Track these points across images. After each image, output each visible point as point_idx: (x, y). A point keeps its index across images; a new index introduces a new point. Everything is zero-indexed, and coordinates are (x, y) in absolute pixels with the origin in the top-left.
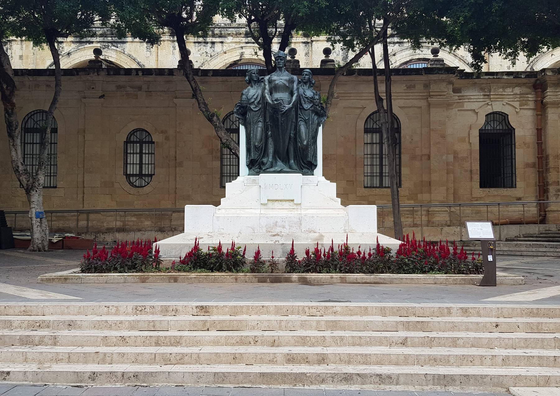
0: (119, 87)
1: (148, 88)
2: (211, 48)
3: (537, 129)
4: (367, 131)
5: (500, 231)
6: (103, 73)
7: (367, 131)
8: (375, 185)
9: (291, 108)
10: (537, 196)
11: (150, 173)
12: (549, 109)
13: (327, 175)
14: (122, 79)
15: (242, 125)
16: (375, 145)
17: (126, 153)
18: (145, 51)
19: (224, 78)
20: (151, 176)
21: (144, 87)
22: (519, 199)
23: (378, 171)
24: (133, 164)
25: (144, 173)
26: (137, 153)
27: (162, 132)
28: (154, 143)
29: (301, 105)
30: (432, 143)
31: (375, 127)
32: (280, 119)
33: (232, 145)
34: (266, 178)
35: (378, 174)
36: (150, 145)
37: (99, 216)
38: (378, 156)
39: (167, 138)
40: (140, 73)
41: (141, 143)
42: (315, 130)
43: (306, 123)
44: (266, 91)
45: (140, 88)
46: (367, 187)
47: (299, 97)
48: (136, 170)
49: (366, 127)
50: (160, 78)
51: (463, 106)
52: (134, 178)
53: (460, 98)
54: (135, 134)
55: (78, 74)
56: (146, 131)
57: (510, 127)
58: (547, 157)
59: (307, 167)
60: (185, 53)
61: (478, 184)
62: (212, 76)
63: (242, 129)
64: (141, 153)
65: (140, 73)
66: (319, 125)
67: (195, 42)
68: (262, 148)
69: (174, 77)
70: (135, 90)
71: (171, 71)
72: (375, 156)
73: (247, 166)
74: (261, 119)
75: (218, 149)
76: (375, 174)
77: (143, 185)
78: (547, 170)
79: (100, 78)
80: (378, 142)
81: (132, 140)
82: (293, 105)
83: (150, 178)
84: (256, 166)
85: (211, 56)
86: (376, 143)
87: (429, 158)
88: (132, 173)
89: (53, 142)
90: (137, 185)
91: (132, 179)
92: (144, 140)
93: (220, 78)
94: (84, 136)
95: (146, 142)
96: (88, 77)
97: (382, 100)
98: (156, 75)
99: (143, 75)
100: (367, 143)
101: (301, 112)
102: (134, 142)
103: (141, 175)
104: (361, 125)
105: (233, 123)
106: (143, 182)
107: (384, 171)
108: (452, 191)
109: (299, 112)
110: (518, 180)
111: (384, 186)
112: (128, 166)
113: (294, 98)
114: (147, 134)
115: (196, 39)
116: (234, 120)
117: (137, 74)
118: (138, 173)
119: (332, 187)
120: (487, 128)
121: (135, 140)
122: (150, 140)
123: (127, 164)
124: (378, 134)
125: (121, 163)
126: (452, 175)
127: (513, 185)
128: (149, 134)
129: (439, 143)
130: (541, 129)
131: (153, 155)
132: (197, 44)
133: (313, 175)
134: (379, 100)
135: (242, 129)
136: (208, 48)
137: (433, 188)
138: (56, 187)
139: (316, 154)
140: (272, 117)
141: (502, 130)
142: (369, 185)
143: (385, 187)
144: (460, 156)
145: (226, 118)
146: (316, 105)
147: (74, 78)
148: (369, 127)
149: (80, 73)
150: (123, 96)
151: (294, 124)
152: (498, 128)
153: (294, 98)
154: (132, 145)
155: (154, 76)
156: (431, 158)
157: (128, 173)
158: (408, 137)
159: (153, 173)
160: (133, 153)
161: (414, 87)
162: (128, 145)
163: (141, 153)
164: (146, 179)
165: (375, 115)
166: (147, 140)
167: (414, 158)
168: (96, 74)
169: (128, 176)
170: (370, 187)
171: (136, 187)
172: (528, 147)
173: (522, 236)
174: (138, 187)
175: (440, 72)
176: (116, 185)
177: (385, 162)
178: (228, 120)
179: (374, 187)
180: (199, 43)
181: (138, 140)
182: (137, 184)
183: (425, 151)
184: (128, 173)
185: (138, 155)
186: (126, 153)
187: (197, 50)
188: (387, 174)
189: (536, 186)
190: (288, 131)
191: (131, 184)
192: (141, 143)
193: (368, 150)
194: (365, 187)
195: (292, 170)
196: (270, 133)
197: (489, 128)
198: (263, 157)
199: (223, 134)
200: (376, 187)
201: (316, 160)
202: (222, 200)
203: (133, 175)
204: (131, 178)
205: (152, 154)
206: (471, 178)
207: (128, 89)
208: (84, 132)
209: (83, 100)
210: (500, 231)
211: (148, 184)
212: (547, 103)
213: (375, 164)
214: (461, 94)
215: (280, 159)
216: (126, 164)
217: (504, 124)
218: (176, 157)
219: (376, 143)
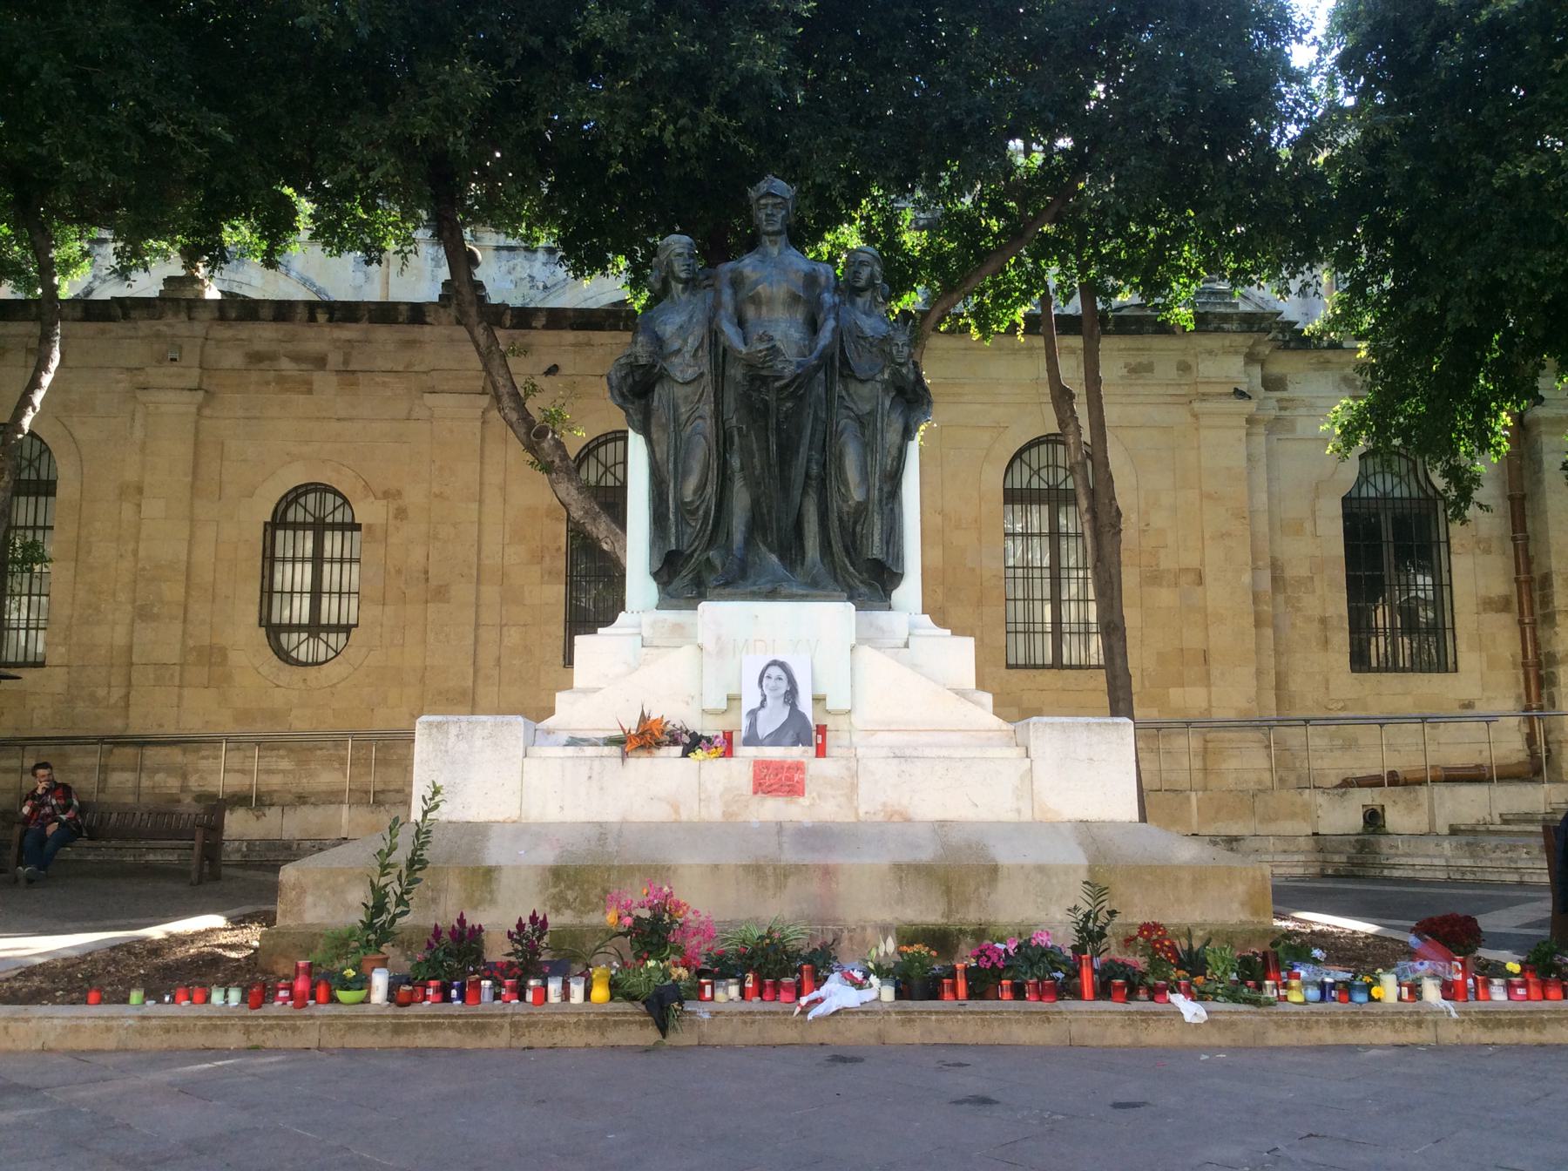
0: (256, 358)
1: (346, 362)
2: (545, 264)
3: (1511, 498)
4: (1012, 497)
5: (1431, 799)
6: (205, 315)
7: (1012, 497)
8: (1039, 662)
9: (817, 369)
10: (1519, 697)
11: (344, 621)
12: (1545, 439)
13: (938, 610)
14: (265, 334)
15: (637, 431)
16: (1036, 540)
17: (270, 559)
18: (351, 269)
19: (582, 335)
20: (347, 629)
21: (335, 359)
22: (1469, 705)
23: (1048, 618)
24: (292, 592)
25: (324, 621)
26: (303, 560)
27: (386, 495)
28: (357, 527)
29: (845, 363)
30: (1207, 536)
31: (1035, 485)
32: (773, 405)
33: (603, 527)
34: (720, 616)
35: (1049, 628)
36: (348, 534)
37: (176, 755)
38: (1047, 573)
39: (401, 514)
40: (322, 317)
41: (319, 527)
42: (894, 452)
43: (862, 425)
44: (722, 312)
45: (320, 362)
46: (1017, 666)
47: (838, 332)
48: (300, 610)
49: (1009, 486)
50: (383, 333)
51: (1292, 429)
52: (295, 636)
53: (1283, 405)
54: (302, 500)
55: (126, 317)
56: (336, 493)
57: (1431, 492)
58: (1546, 581)
59: (871, 580)
60: (462, 261)
61: (1345, 660)
62: (546, 327)
63: (637, 447)
64: (318, 560)
65: (322, 317)
66: (907, 434)
67: (498, 248)
68: (707, 513)
69: (427, 328)
70: (304, 366)
71: (417, 313)
72: (1037, 573)
73: (656, 575)
74: (707, 409)
75: (559, 549)
76: (1038, 628)
77: (322, 658)
78: (1549, 619)
79: (198, 328)
80: (1046, 530)
81: (290, 517)
82: (820, 357)
83: (343, 636)
84: (686, 576)
85: (545, 287)
86: (1040, 535)
87: (1200, 580)
89: (40, 522)
90: (302, 658)
91: (289, 640)
92: (329, 519)
93: (570, 336)
94: (139, 506)
95: (334, 527)
96: (160, 326)
97: (1071, 396)
98: (371, 321)
99: (330, 320)
100: (1014, 535)
101: (846, 389)
102: (296, 526)
103: (315, 627)
104: (994, 480)
105: (607, 469)
106: (322, 647)
107: (1065, 620)
108: (1271, 679)
109: (839, 387)
110: (1462, 646)
111: (1065, 661)
113: (825, 337)
114: (339, 501)
115: (502, 240)
116: (610, 462)
117: (312, 319)
118: (305, 620)
119: (956, 656)
120: (1364, 494)
121: (300, 518)
122: (348, 519)
123: (271, 592)
124: (1045, 509)
125: (253, 590)
126: (1269, 632)
127: (1442, 663)
128: (346, 501)
129: (1229, 534)
130: (1524, 497)
131: (355, 567)
132: (505, 253)
133: (890, 608)
134: (1062, 398)
135: (637, 447)
136: (538, 265)
137: (1215, 672)
138: (42, 665)
139: (901, 537)
140: (745, 400)
141: (1411, 498)
142: (1021, 661)
143: (1071, 667)
144: (1290, 573)
145: (587, 455)
146: (901, 365)
147: (116, 328)
148: (1017, 486)
149: (134, 314)
150: (268, 383)
151: (820, 428)
152: (1397, 494)
153: (825, 337)
154: (290, 533)
155: (364, 325)
156: (1208, 579)
157: (275, 620)
158: (1134, 517)
159: (352, 621)
160: (294, 560)
161: (1148, 368)
162: (280, 534)
163: (318, 560)
164: (333, 638)
165: (1034, 451)
166: (338, 517)
167: (1154, 578)
168: (183, 316)
169: (274, 631)
170: (1026, 667)
171: (298, 663)
172: (1487, 551)
173: (1497, 820)
174: (306, 664)
175: (1225, 326)
176: (235, 657)
177: (1071, 589)
178: (592, 461)
179: (1035, 667)
180: (511, 249)
181: (310, 519)
182: (302, 654)
183: (1191, 560)
184: (275, 620)
185: (308, 567)
186: (270, 559)
187: (504, 269)
188: (1075, 628)
189: (1515, 665)
190: (803, 450)
191: (284, 656)
192: (319, 527)
193: (1015, 550)
194: (1008, 666)
195: (813, 589)
196: (736, 462)
197: (1372, 493)
198: (710, 544)
199: (574, 492)
200: (1044, 666)
201: (899, 558)
202: (561, 698)
203: (291, 628)
204: (284, 637)
205: (351, 561)
206: (1326, 642)
207: (286, 365)
208: (140, 490)
209: (139, 394)
210: (1431, 799)
211: (337, 654)
212: (1537, 422)
213: (1038, 595)
214: (1284, 394)
215: (771, 550)
216: (268, 592)
217: (1414, 485)
218: (426, 572)
219: (1040, 535)
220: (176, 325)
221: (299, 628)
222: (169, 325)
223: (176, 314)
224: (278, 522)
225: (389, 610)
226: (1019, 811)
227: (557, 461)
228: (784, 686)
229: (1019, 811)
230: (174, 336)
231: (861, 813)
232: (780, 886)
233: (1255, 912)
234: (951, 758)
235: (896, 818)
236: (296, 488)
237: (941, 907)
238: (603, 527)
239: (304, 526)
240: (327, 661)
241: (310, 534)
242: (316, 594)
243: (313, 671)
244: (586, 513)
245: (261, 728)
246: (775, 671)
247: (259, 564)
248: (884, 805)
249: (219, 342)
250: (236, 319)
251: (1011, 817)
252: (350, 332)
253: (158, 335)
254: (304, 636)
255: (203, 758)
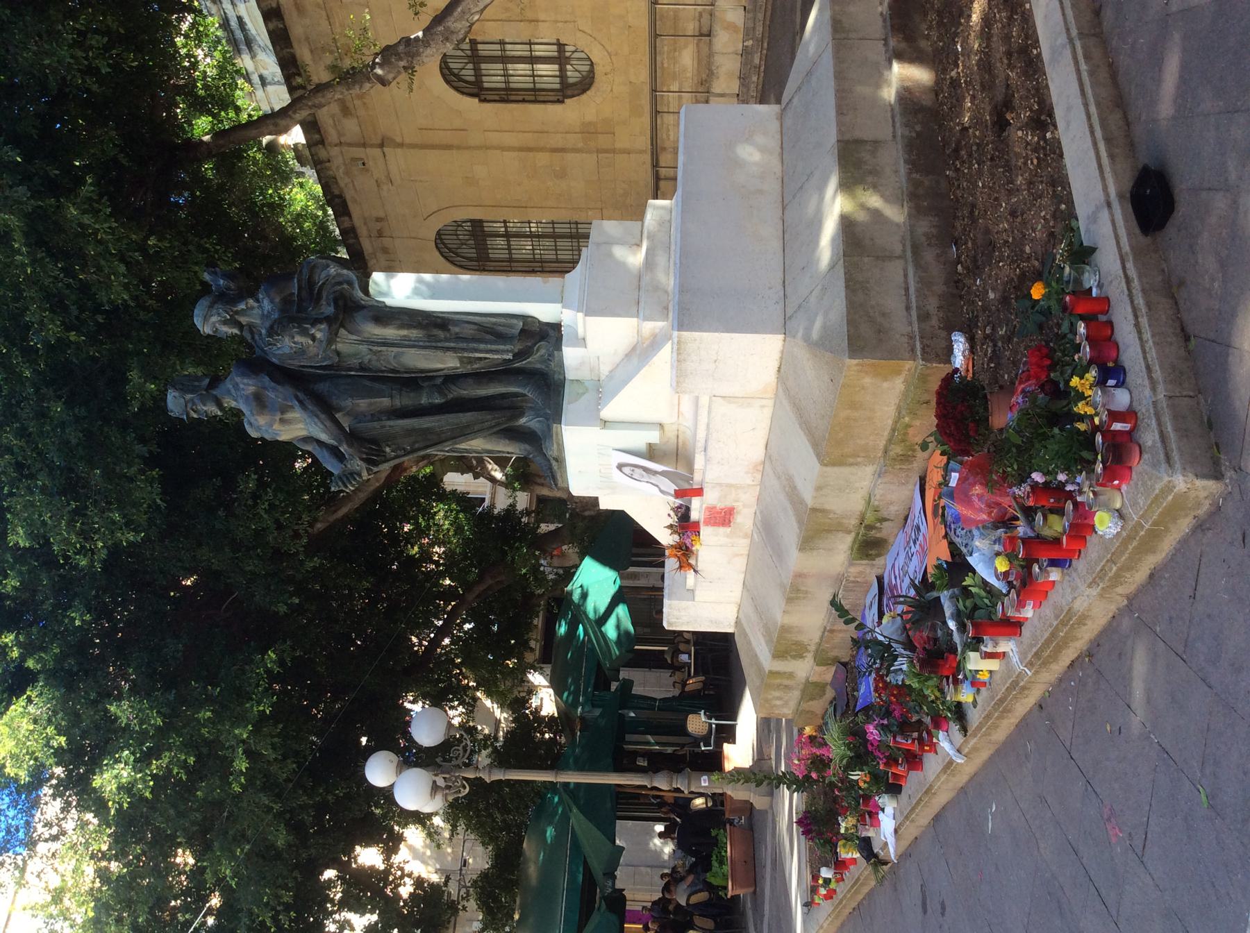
26: (505, 69)
33: (458, 25)
41: (476, 58)
50: (297, 28)
79: (335, 151)
81: (472, 79)
88: (558, 80)
91: (572, 75)
96: (340, 174)
102: (478, 74)
112: (538, 86)
118: (556, 67)
147: (349, 195)
162: (486, 85)
184: (557, 86)
186: (507, 95)
203: (562, 75)
204: (571, 81)
216: (535, 95)
220: (337, 159)
221: (562, 70)
222: (338, 168)
223: (328, 169)
224: (477, 90)
225: (542, 16)
226: (763, 407)
227: (402, 64)
228: (641, 471)
229: (763, 407)
230: (345, 164)
231: (749, 482)
232: (806, 592)
233: (898, 373)
234: (708, 425)
235: (761, 468)
236: (448, 82)
237: (840, 535)
238: (458, 25)
239: (477, 70)
240: (589, 59)
241: (483, 66)
242: (533, 60)
243: (597, 69)
244: (447, 39)
245: (645, 101)
246: (627, 470)
247: (514, 105)
248: (747, 473)
249: (340, 135)
250: (319, 132)
251: (768, 412)
252: (303, 53)
253: (347, 173)
254: (569, 67)
255: (668, 136)
